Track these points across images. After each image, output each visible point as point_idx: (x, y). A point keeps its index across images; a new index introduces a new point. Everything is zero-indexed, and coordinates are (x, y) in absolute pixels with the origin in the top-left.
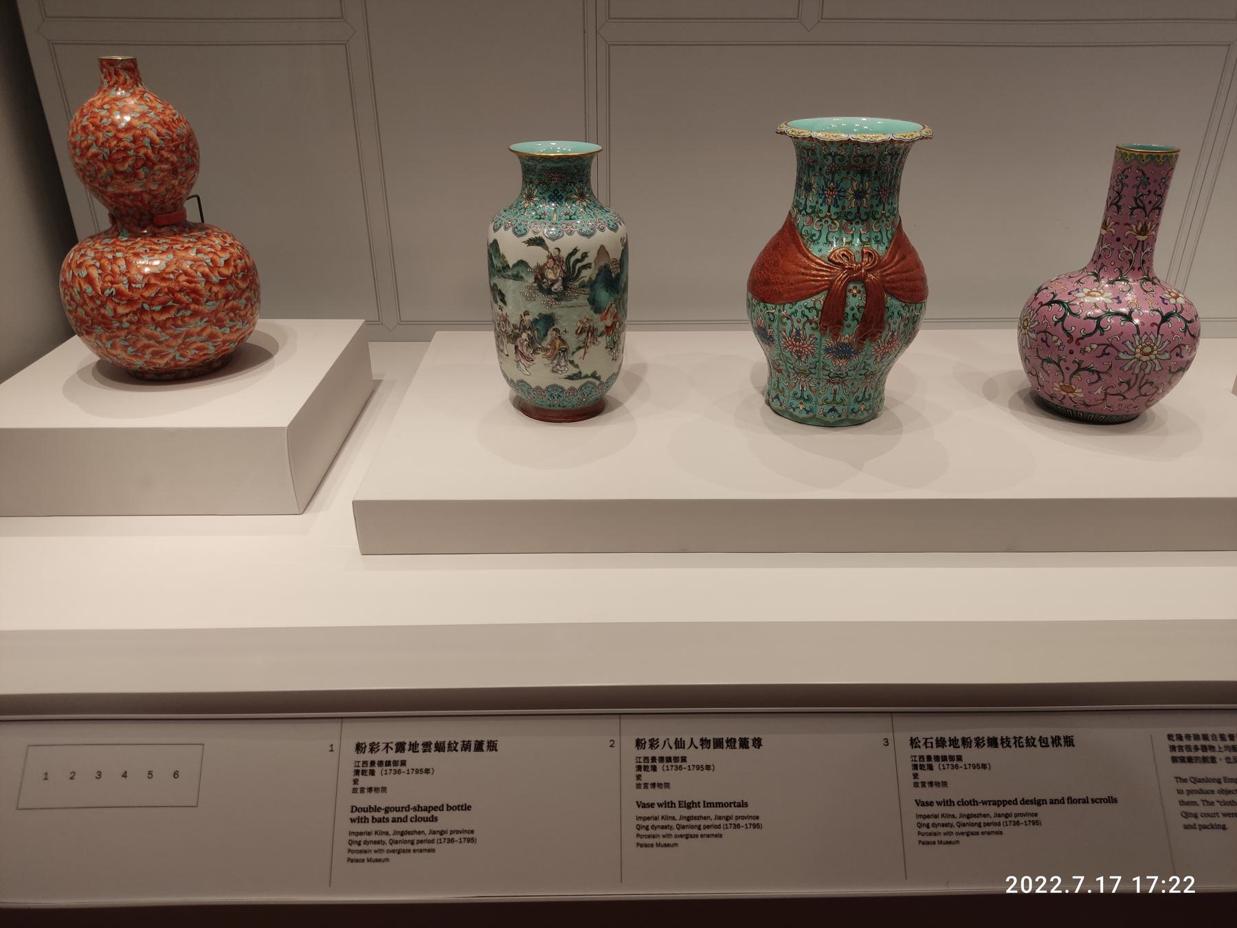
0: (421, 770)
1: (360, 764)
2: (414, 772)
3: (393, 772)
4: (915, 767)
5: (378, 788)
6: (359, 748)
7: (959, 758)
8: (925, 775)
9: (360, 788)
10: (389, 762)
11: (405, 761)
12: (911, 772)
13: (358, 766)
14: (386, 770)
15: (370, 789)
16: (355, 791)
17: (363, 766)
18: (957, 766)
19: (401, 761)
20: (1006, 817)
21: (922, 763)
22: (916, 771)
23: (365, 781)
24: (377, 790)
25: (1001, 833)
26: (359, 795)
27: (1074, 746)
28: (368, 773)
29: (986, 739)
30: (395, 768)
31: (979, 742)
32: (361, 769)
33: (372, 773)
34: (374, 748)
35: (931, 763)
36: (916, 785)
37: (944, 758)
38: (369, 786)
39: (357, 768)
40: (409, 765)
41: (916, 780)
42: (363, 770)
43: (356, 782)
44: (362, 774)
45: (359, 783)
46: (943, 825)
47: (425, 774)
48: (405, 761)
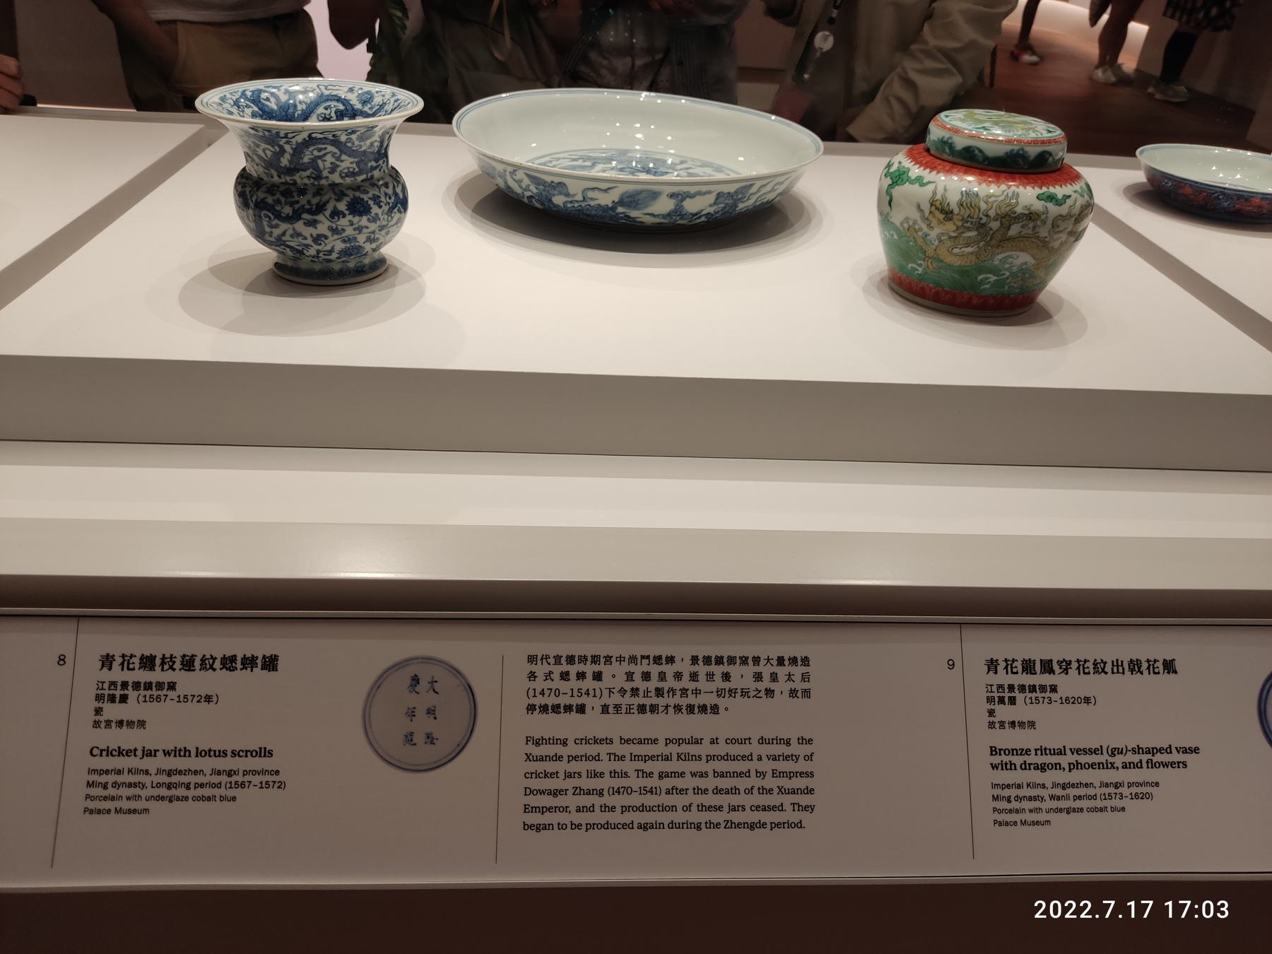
1: (106, 686)
6: (107, 661)
13: (102, 689)
14: (145, 696)
16: (96, 724)
17: (109, 690)
19: (168, 683)
23: (113, 711)
24: (130, 724)
26: (102, 731)
30: (160, 692)
33: (124, 699)
34: (126, 662)
36: (991, 725)
38: (119, 719)
39: (100, 692)
40: (180, 690)
41: (991, 719)
43: (98, 711)
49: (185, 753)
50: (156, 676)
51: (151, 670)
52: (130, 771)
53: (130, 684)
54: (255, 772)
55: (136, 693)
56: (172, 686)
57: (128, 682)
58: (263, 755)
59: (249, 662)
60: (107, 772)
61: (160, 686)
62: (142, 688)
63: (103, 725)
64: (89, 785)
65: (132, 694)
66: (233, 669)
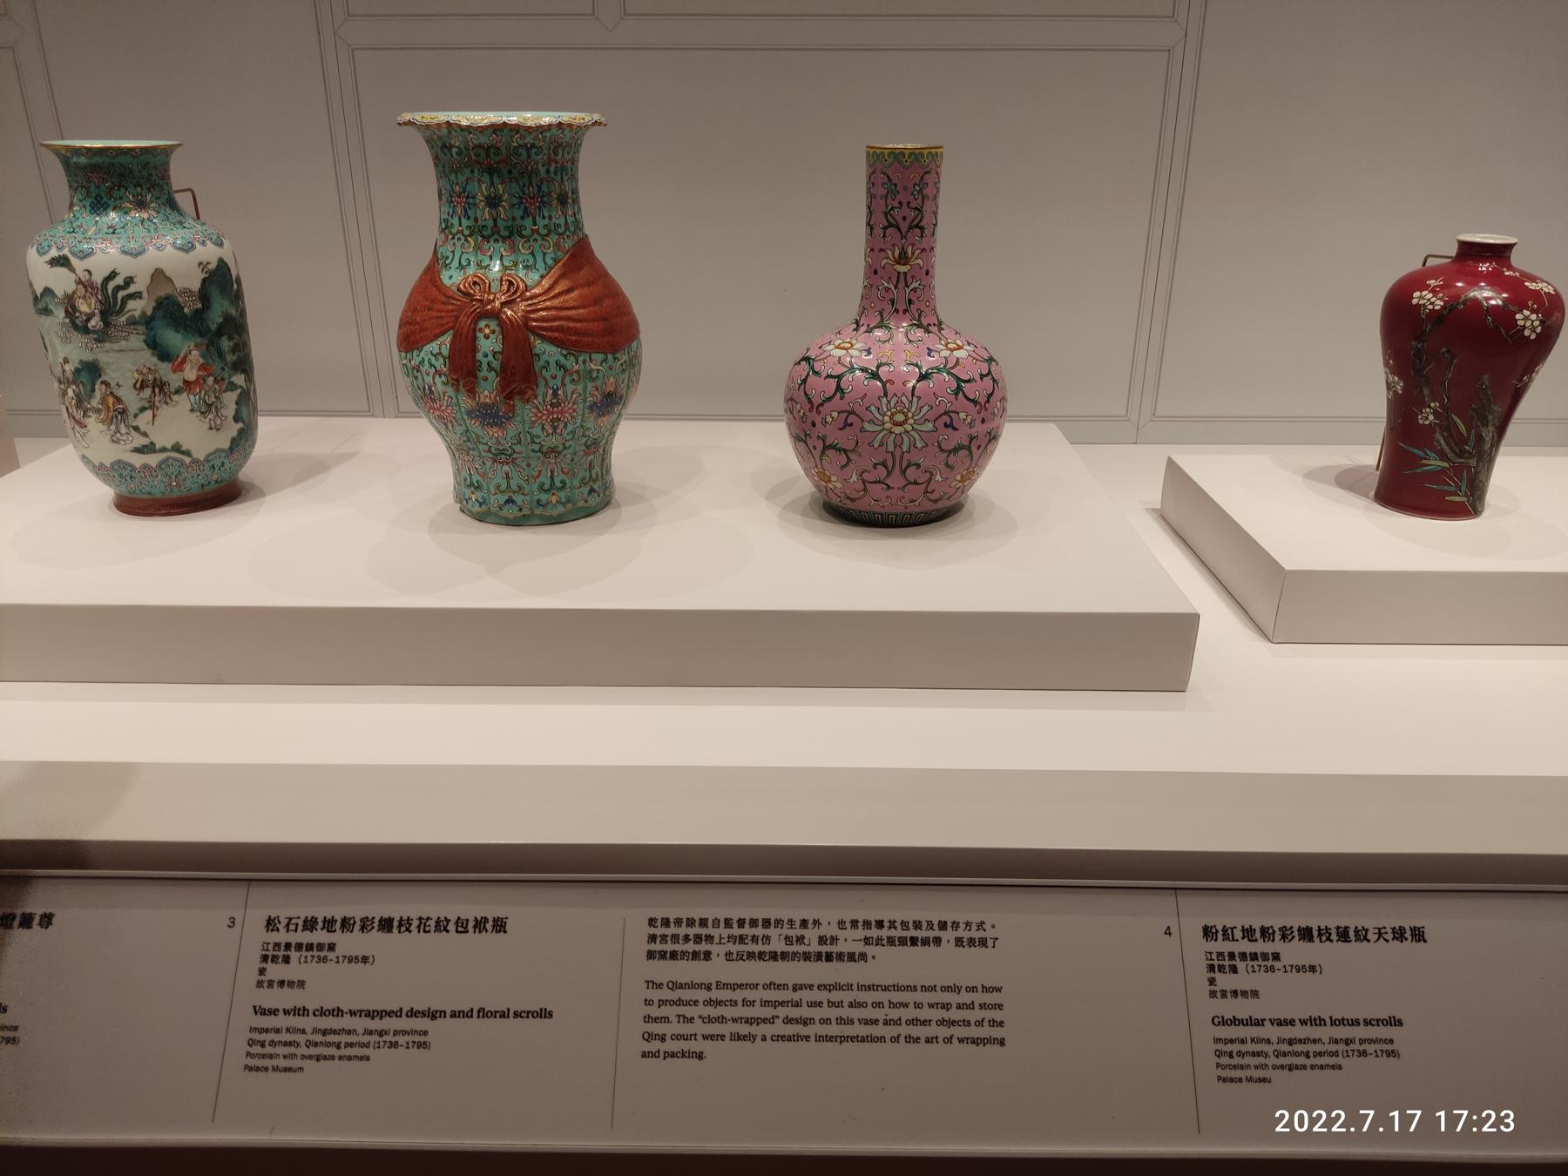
0: (357, 957)
1: (271, 947)
2: (347, 960)
3: (316, 959)
4: (1211, 968)
5: (293, 982)
7: (1276, 957)
8: (1225, 981)
9: (268, 981)
10: (312, 944)
11: (334, 945)
12: (1205, 975)
13: (268, 950)
14: (306, 957)
15: (282, 983)
16: (260, 984)
17: (274, 950)
18: (1272, 967)
19: (329, 944)
20: (1347, 1044)
21: (1221, 963)
22: (1212, 975)
23: (275, 971)
24: (291, 984)
25: (1340, 1067)
26: (265, 991)
27: (1425, 941)
28: (280, 960)
29: (1295, 929)
30: (320, 953)
31: (1306, 934)
32: (270, 953)
33: (287, 960)
35: (1234, 962)
36: (1213, 994)
37: (1254, 957)
39: (264, 953)
42: (273, 956)
43: (262, 971)
44: (272, 961)
45: (267, 973)
46: (1254, 1054)
47: (363, 964)
48: (334, 945)
49: (338, 1012)
50: (320, 936)
51: (388, 932)
52: (288, 1030)
53: (293, 945)
54: (405, 1033)
55: (298, 954)
56: (332, 947)
57: (291, 943)
58: (543, 1015)
59: (480, 925)
60: (267, 1031)
61: (320, 947)
62: (304, 949)
63: (265, 985)
64: (251, 1043)
65: (294, 955)
66: (390, 930)
